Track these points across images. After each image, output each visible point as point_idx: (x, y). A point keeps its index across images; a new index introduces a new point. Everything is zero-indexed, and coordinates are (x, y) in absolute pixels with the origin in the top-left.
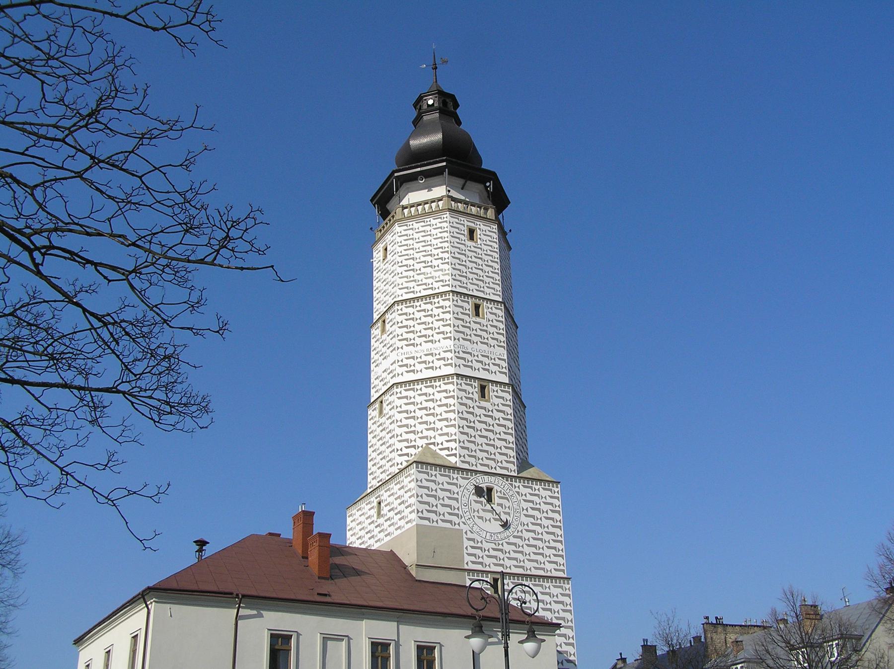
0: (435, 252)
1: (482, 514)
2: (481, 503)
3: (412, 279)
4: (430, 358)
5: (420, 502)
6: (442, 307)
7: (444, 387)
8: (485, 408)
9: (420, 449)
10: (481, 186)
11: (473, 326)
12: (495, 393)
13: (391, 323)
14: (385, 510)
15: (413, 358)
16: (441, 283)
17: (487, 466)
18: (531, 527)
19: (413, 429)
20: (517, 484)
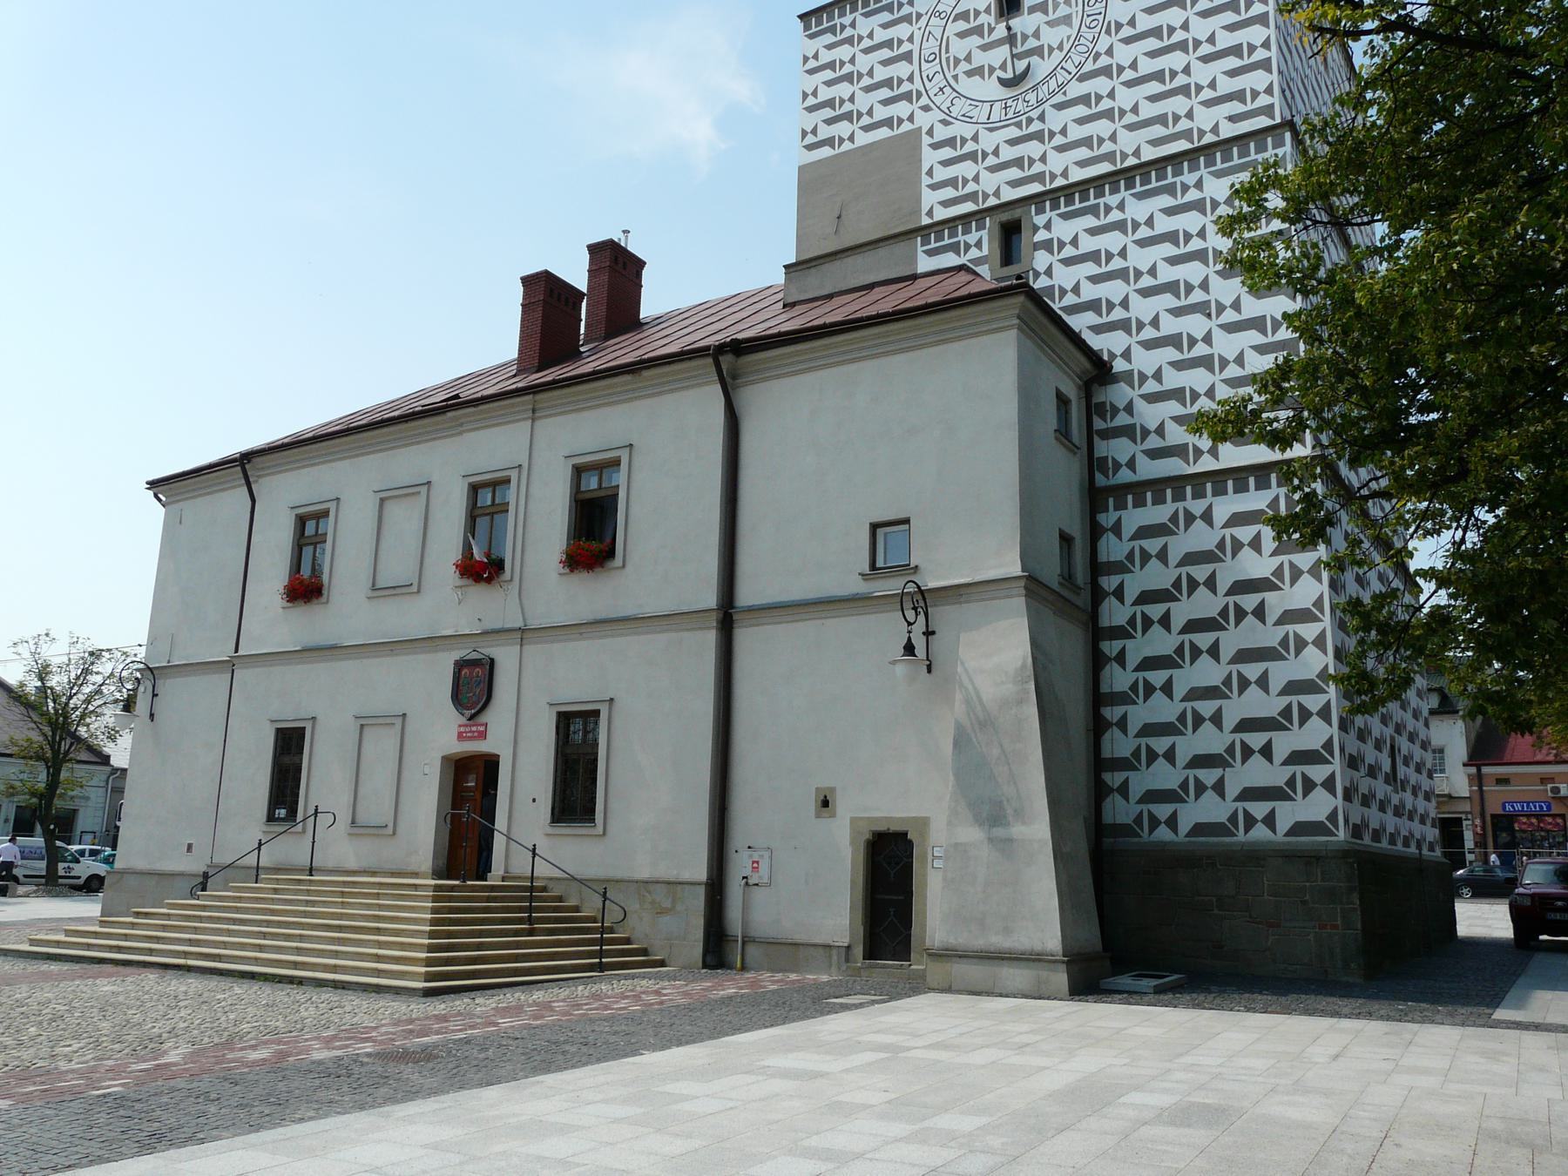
1: (980, 59)
2: (978, 31)
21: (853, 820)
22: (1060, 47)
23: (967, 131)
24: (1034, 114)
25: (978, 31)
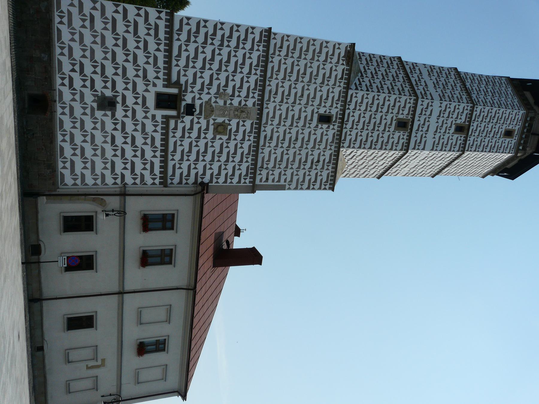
8: (391, 124)
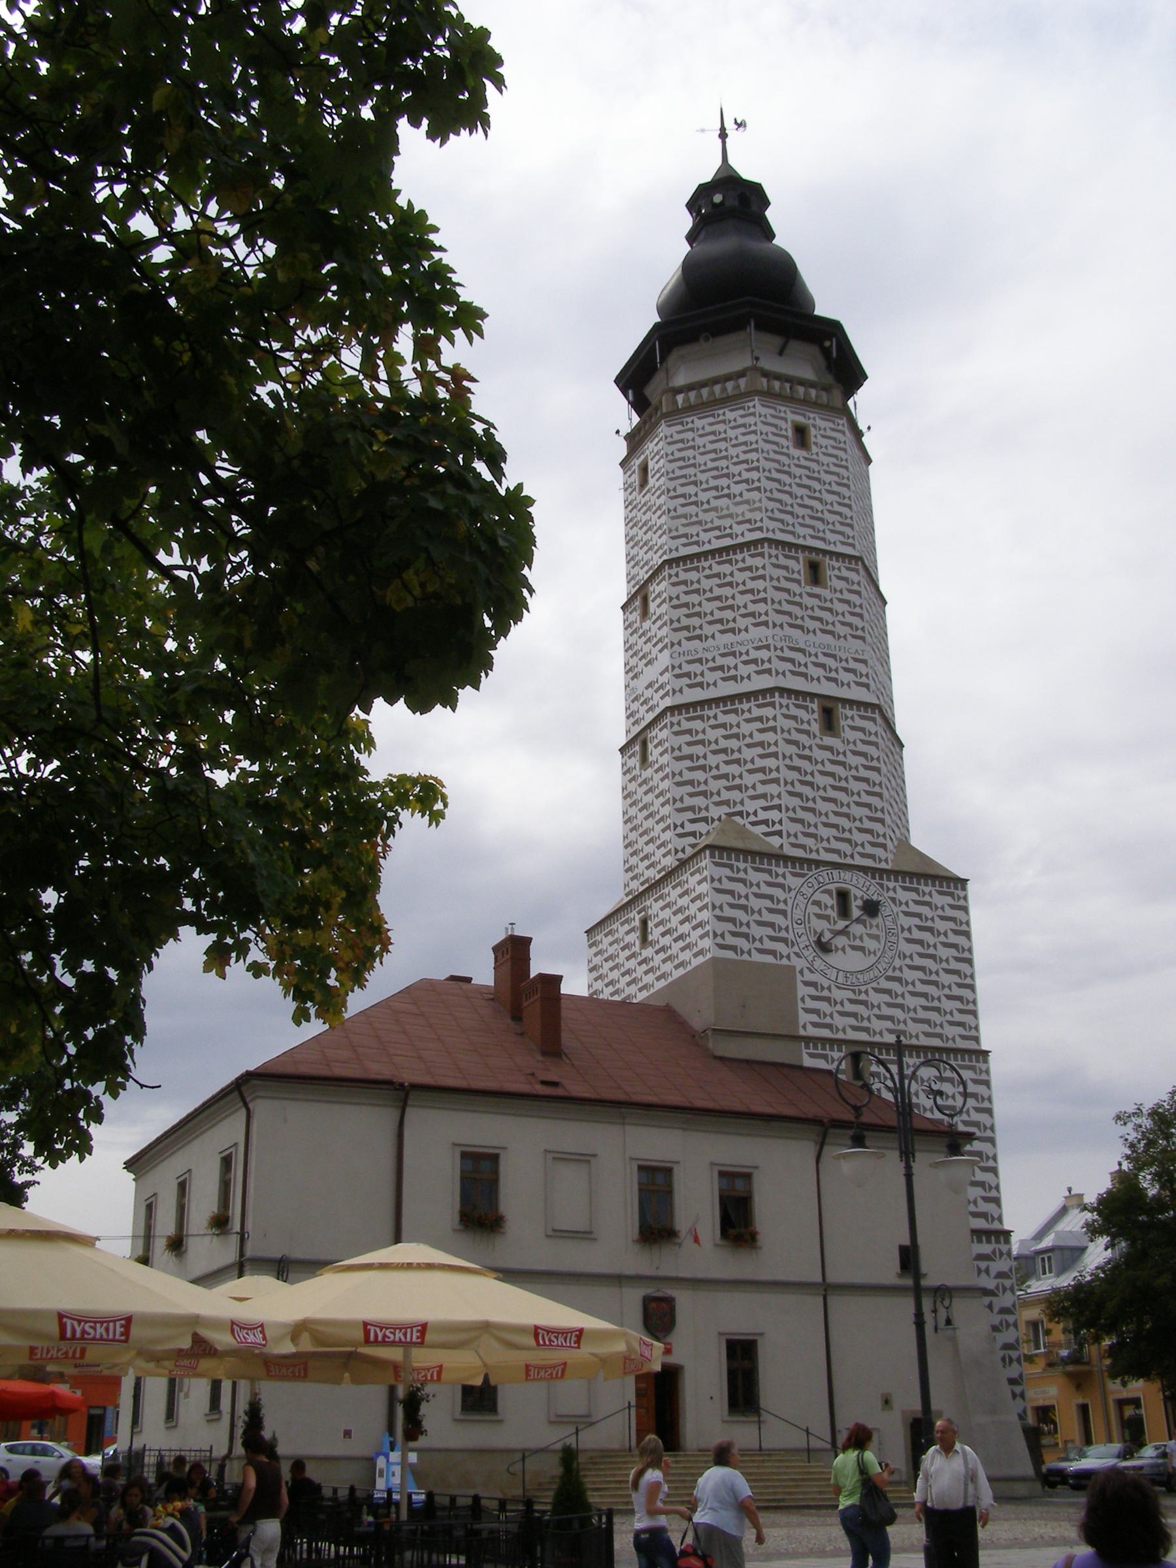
0: (735, 469)
2: (827, 918)
3: (694, 519)
4: (730, 661)
5: (719, 918)
6: (750, 569)
7: (756, 712)
8: (830, 749)
9: (716, 823)
10: (814, 350)
11: (808, 601)
12: (849, 722)
13: (659, 601)
14: (655, 933)
15: (700, 661)
16: (748, 526)
17: (837, 852)
18: (918, 961)
19: (702, 788)
20: (891, 885)
21: (903, 1412)
22: (874, 953)
23: (826, 984)
24: (863, 988)
25: (827, 918)
